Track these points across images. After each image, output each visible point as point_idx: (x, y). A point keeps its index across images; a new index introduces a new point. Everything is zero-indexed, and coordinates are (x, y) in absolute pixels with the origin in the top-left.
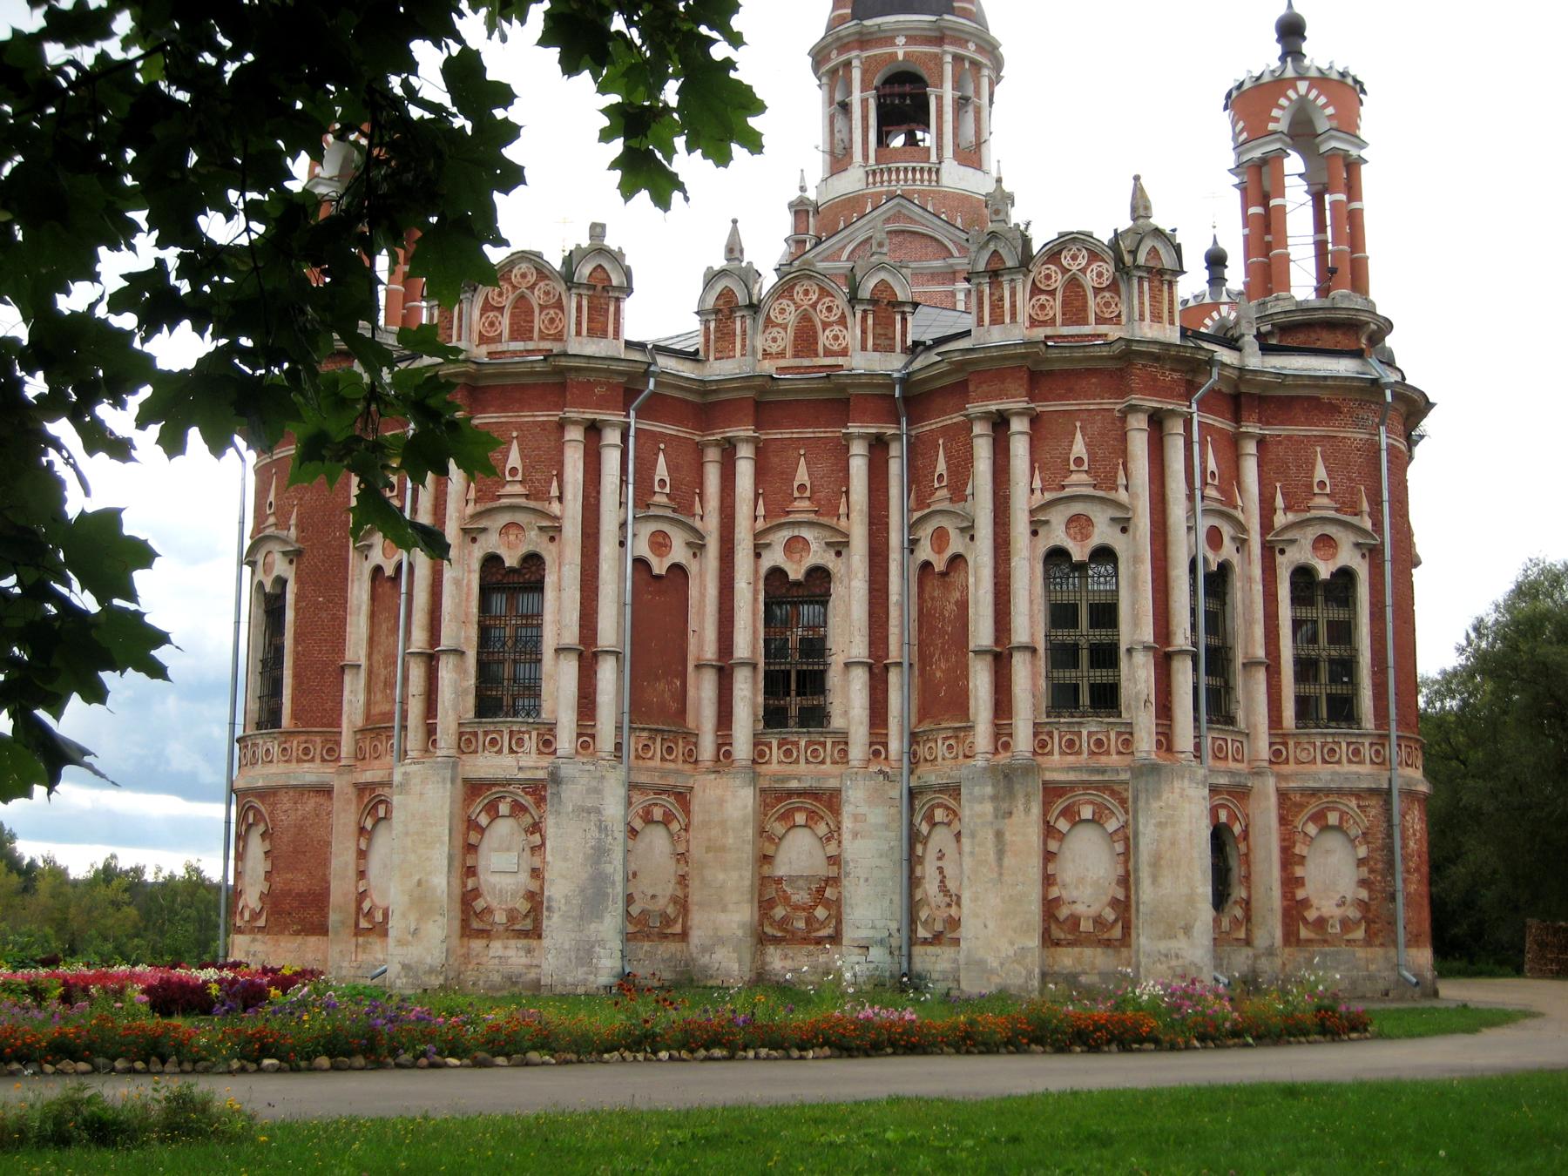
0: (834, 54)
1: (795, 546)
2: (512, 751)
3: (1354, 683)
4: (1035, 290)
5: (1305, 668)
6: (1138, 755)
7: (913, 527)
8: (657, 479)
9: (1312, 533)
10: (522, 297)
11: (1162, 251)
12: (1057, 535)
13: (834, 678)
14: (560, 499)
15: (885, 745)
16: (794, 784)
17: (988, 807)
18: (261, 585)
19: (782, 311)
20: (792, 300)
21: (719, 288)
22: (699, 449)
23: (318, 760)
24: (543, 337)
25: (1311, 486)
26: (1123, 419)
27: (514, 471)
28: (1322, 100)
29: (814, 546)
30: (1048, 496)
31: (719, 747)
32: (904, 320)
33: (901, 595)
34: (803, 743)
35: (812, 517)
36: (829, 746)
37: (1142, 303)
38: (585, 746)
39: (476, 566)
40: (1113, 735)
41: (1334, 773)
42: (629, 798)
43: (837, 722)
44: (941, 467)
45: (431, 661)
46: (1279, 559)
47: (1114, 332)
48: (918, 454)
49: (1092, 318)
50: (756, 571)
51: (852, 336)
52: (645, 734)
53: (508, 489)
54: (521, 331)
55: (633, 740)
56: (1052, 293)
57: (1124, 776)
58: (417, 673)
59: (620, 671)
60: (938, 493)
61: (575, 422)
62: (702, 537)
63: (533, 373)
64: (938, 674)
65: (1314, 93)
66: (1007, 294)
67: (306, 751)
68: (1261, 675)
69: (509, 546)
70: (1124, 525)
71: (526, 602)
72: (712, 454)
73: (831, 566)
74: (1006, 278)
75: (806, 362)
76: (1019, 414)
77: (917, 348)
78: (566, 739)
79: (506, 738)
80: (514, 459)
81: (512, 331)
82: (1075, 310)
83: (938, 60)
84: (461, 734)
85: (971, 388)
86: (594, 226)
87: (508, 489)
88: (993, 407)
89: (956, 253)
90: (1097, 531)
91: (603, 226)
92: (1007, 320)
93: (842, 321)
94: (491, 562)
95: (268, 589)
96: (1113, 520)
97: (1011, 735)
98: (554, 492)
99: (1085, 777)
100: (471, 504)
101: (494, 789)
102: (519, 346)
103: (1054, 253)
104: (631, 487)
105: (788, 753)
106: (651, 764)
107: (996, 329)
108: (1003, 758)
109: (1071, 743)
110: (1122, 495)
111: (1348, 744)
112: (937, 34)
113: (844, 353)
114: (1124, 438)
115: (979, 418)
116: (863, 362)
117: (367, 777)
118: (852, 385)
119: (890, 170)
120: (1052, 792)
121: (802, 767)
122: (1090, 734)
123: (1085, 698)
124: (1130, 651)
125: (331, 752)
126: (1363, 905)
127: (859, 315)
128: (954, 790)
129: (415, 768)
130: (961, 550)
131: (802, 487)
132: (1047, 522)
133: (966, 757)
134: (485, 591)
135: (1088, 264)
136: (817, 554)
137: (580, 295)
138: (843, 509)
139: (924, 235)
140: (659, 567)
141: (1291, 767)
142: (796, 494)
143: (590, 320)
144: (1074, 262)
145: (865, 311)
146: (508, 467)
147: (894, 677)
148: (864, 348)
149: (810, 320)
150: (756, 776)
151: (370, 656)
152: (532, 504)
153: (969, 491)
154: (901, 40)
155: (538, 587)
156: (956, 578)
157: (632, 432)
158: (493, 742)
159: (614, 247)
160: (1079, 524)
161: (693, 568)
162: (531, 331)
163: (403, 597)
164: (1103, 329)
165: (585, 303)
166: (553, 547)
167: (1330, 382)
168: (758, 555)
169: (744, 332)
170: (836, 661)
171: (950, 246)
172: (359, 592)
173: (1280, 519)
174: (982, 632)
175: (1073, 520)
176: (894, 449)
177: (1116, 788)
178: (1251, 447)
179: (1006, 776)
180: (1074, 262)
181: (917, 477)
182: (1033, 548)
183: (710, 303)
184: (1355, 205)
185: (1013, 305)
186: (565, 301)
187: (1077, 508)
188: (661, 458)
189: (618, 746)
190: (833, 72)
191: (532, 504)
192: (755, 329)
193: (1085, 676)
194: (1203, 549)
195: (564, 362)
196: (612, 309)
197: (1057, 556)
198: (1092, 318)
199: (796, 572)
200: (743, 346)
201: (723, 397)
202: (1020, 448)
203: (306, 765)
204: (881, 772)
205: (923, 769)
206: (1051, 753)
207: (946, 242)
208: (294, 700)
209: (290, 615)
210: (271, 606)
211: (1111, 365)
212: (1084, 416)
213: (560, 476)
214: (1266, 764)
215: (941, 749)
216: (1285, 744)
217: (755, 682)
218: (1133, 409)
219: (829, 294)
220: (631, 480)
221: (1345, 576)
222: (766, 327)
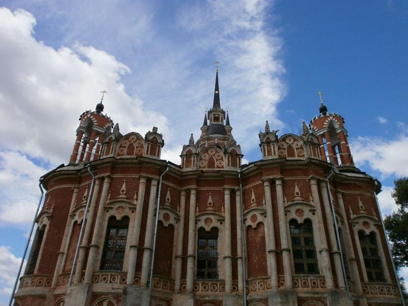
1: (208, 221)
2: (110, 282)
3: (382, 269)
4: (279, 148)
5: (367, 261)
6: (327, 287)
7: (245, 215)
8: (167, 198)
9: (361, 221)
10: (132, 144)
11: (314, 139)
12: (293, 215)
13: (219, 262)
14: (137, 200)
15: (237, 285)
16: (207, 298)
18: (38, 228)
19: (205, 156)
20: (208, 153)
22: (179, 192)
23: (43, 286)
25: (358, 207)
26: (309, 182)
27: (123, 191)
28: (336, 121)
29: (214, 221)
30: (289, 203)
31: (181, 285)
32: (239, 160)
33: (242, 236)
34: (210, 284)
35: (213, 212)
36: (218, 285)
37: (311, 151)
38: (137, 281)
39: (107, 219)
40: (318, 280)
41: (385, 298)
42: (151, 301)
43: (221, 277)
44: (253, 197)
45: (87, 249)
46: (354, 228)
48: (246, 195)
49: (296, 155)
50: (196, 228)
51: (225, 162)
52: (158, 279)
53: (121, 196)
54: (130, 152)
55: (153, 280)
56: (284, 149)
57: (326, 295)
58: (82, 253)
59: (151, 256)
60: (252, 205)
61: (144, 177)
62: (179, 217)
63: (133, 163)
64: (255, 261)
65: (334, 119)
66: (272, 148)
67: (40, 282)
68: (355, 264)
69: (119, 213)
70: (313, 212)
71: (121, 232)
72: (183, 193)
73: (219, 227)
74: (272, 144)
75: (212, 169)
76: (279, 179)
78: (129, 279)
79: (109, 277)
80: (124, 187)
81: (127, 153)
84: (94, 276)
85: (263, 173)
86: (154, 128)
87: (121, 196)
90: (305, 214)
91: (157, 128)
92: (273, 154)
93: (222, 159)
94: (112, 218)
95: (40, 229)
97: (284, 280)
98: (135, 197)
99: (312, 296)
100: (108, 200)
101: (104, 296)
102: (129, 157)
103: (284, 139)
104: (159, 199)
105: (205, 287)
106: (159, 289)
108: (282, 288)
109: (305, 283)
110: (312, 203)
111: (386, 288)
113: (223, 167)
114: (310, 187)
115: (266, 181)
117: (58, 292)
118: (226, 174)
121: (210, 292)
122: (311, 280)
123: (306, 268)
124: (320, 252)
125: (49, 283)
127: (227, 157)
129: (75, 287)
130: (261, 221)
131: (210, 204)
132: (289, 211)
133: (268, 288)
134: (109, 227)
135: (294, 142)
136: (214, 223)
137: (149, 144)
138: (222, 210)
140: (166, 224)
141: (369, 296)
142: (208, 205)
143: (151, 151)
144: (290, 141)
145: (229, 156)
146: (122, 189)
147: (239, 262)
148: (229, 165)
149: (213, 159)
150: (194, 296)
151: (68, 250)
152: (128, 201)
153: (264, 202)
154: (216, 139)
155: (126, 227)
156: (260, 230)
157: (161, 183)
158: (105, 279)
159: (159, 133)
161: (176, 226)
163: (82, 229)
164: (300, 158)
165: (150, 146)
166: (132, 214)
167: (360, 179)
168: (196, 223)
169: (194, 161)
170: (220, 257)
172: (69, 229)
173: (352, 216)
174: (270, 245)
175: (297, 211)
176: (238, 193)
177: (322, 300)
178: (340, 196)
179: (285, 295)
180: (290, 141)
181: (246, 202)
182: (286, 219)
183: (185, 153)
184: (347, 145)
187: (298, 207)
188: (168, 193)
189: (148, 282)
191: (128, 201)
192: (197, 160)
193: (305, 261)
195: (142, 159)
196: (158, 148)
197: (293, 222)
198: (296, 155)
199: (208, 228)
200: (194, 164)
201: (188, 177)
202: (279, 189)
203: (39, 288)
204: (237, 294)
205: (251, 293)
206: (298, 287)
208: (40, 264)
209: (45, 236)
210: (40, 233)
211: (304, 167)
212: (297, 181)
213: (137, 193)
214: (362, 294)
215: (258, 286)
216: (366, 287)
217: (194, 263)
218: (313, 178)
219: (218, 152)
220: (159, 196)
221: (372, 233)
222: (200, 160)
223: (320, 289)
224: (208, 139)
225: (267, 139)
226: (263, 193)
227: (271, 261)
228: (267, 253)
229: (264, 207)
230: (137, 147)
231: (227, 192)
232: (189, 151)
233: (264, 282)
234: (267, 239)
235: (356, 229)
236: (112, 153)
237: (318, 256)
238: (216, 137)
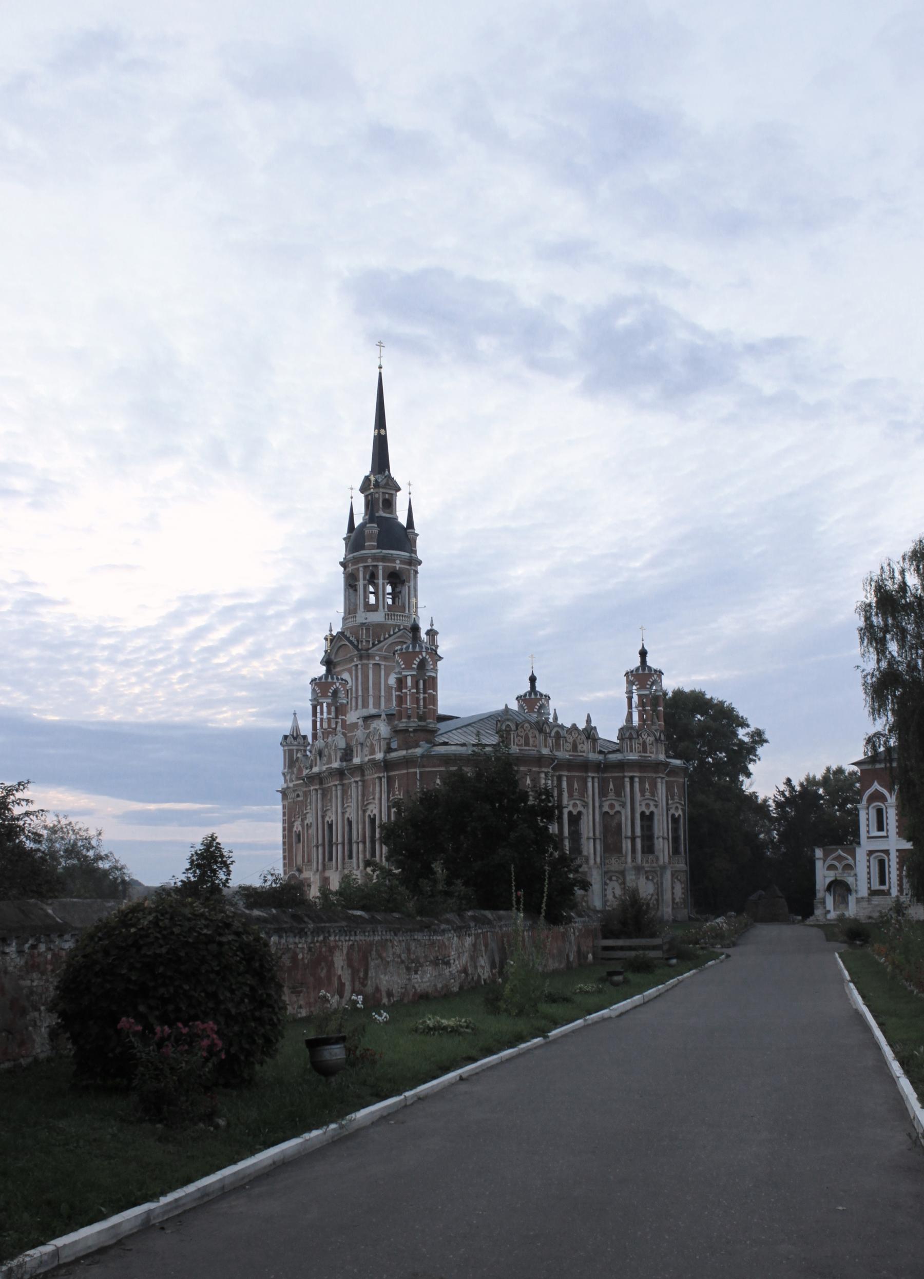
0: (370, 560)
9: (674, 806)
12: (644, 809)
13: (584, 841)
17: (634, 877)
21: (555, 730)
43: (585, 853)
44: (611, 786)
47: (653, 756)
70: (656, 806)
77: (601, 752)
82: (645, 751)
83: (409, 570)
88: (631, 774)
116: (593, 757)
120: (646, 872)
126: (683, 899)
128: (623, 873)
136: (580, 808)
154: (398, 562)
160: (648, 805)
173: (670, 802)
174: (627, 831)
187: (647, 801)
190: (365, 567)
199: (575, 813)
202: (637, 786)
215: (613, 861)
223: (655, 865)
224: (384, 559)
225: (627, 733)
226: (623, 786)
227: (627, 845)
229: (623, 799)
231: (590, 780)
232: (557, 732)
234: (623, 826)
235: (670, 813)
237: (656, 841)
238: (399, 557)
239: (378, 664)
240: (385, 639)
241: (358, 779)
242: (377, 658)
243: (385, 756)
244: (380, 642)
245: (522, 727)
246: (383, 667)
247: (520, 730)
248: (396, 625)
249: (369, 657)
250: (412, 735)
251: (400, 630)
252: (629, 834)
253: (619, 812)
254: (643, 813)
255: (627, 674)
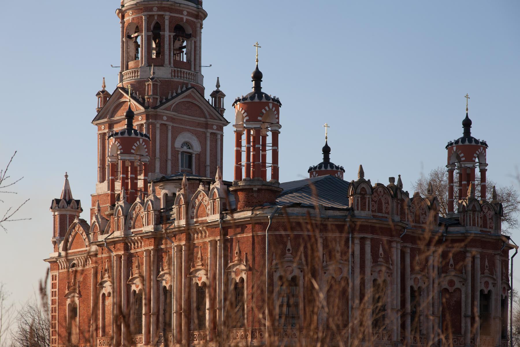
12: (483, 287)
24: (386, 213)
49: (488, 227)
66: (476, 218)
70: (494, 285)
82: (485, 225)
89: (208, 116)
96: (492, 283)
98: (391, 262)
107: (474, 227)
110: (495, 277)
112: (196, 13)
119: (181, 71)
124: (494, 319)
130: (459, 287)
139: (196, 104)
160: (487, 283)
162: (382, 209)
171: (206, 113)
185: (478, 221)
186: (390, 202)
194: (483, 287)
207: (205, 111)
228: (462, 316)
230: (385, 203)
233: (457, 339)
234: (463, 305)
236: (369, 210)
239: (165, 125)
240: (173, 98)
241: (122, 253)
242: (165, 118)
243: (222, 218)
244: (168, 100)
245: (376, 192)
246: (170, 128)
247: (375, 194)
248: (183, 83)
249: (156, 117)
250: (255, 195)
251: (187, 89)
252: (469, 313)
253: (459, 290)
254: (482, 291)
255: (449, 146)
